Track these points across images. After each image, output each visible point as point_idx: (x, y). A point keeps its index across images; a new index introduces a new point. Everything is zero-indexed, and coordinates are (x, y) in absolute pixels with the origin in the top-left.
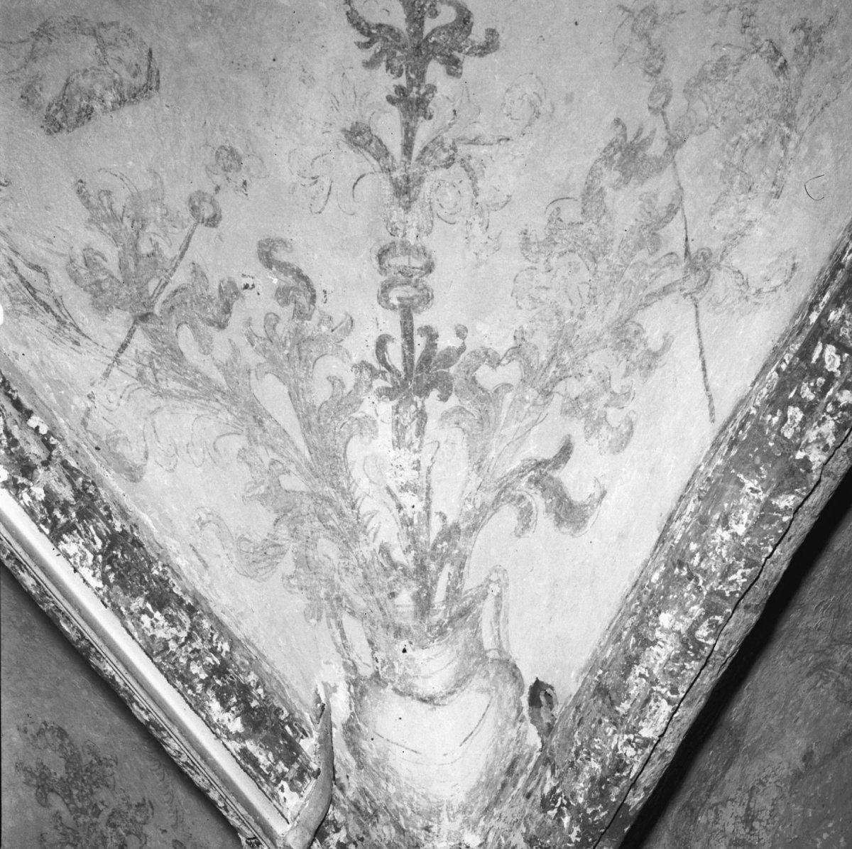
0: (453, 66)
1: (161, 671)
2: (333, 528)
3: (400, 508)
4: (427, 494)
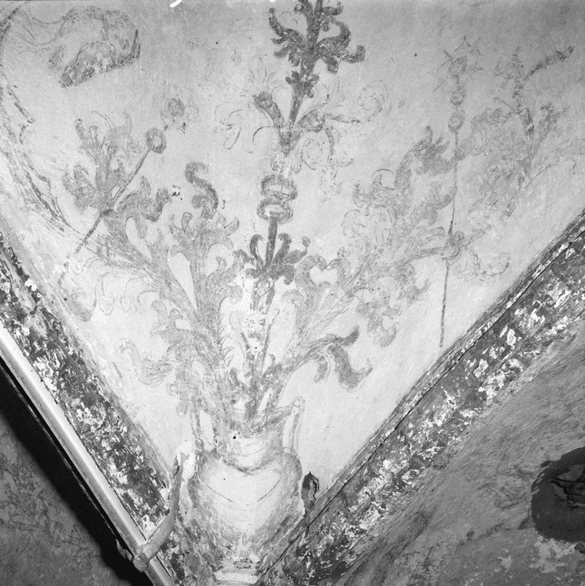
0: (332, 65)
1: (84, 444)
2: (204, 355)
3: (248, 347)
4: (266, 341)
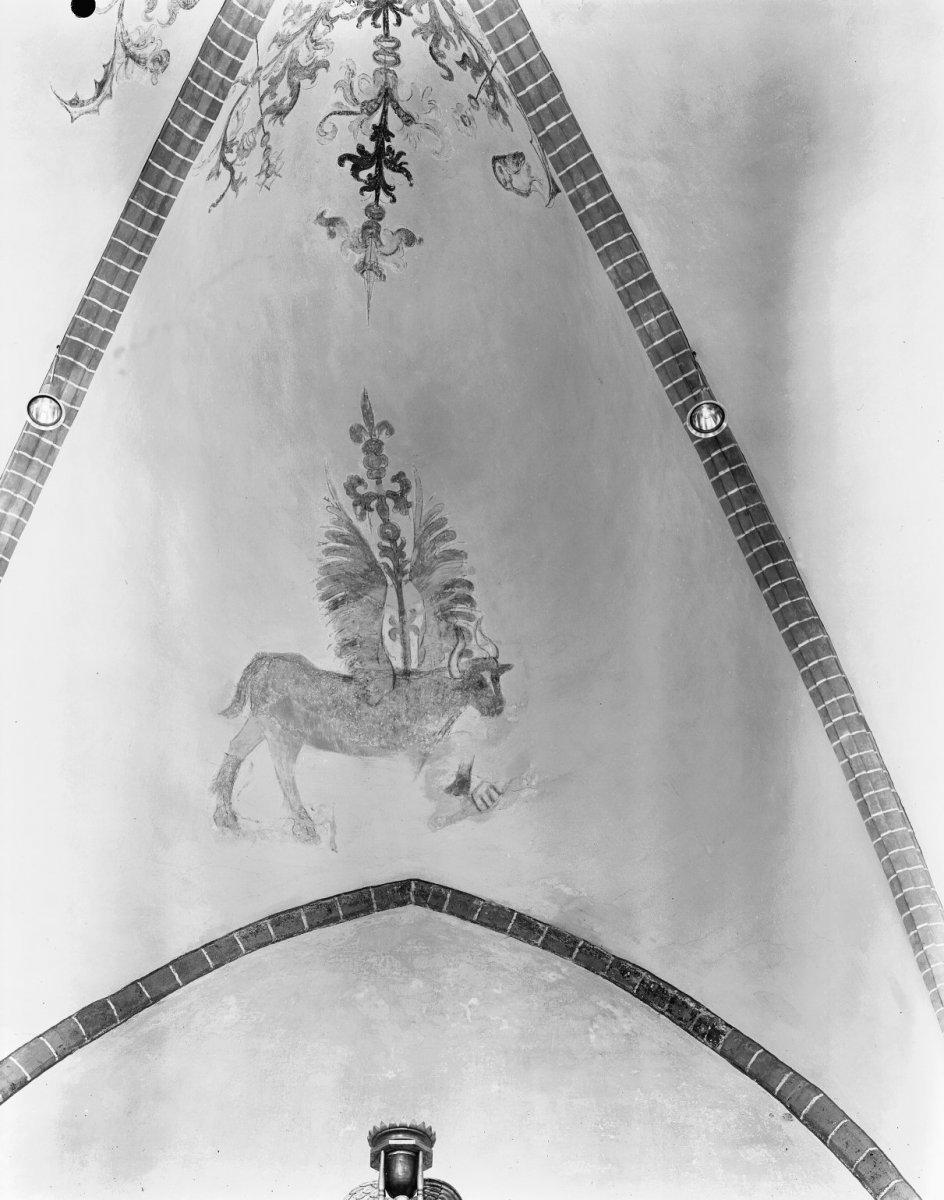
0: (361, 149)
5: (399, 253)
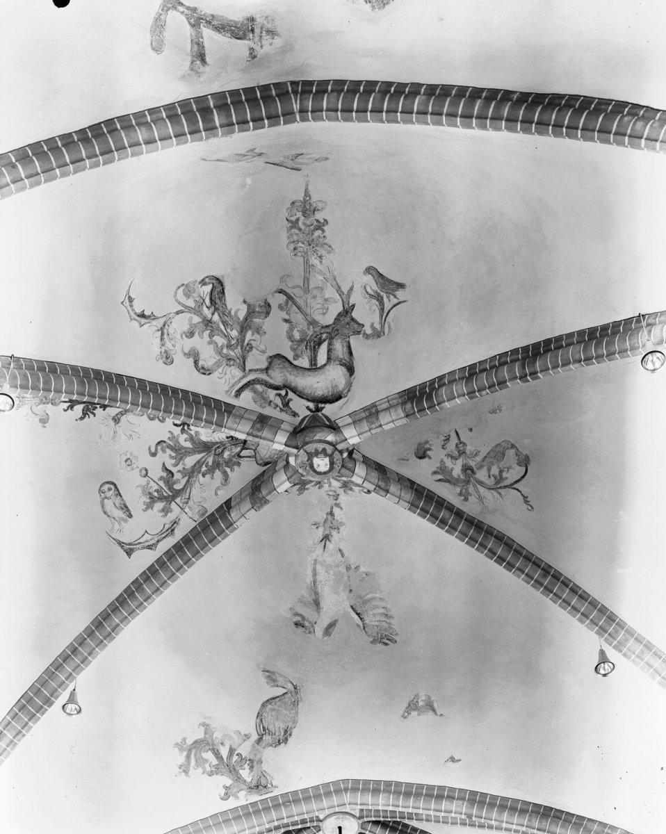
5: (34, 416)
